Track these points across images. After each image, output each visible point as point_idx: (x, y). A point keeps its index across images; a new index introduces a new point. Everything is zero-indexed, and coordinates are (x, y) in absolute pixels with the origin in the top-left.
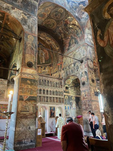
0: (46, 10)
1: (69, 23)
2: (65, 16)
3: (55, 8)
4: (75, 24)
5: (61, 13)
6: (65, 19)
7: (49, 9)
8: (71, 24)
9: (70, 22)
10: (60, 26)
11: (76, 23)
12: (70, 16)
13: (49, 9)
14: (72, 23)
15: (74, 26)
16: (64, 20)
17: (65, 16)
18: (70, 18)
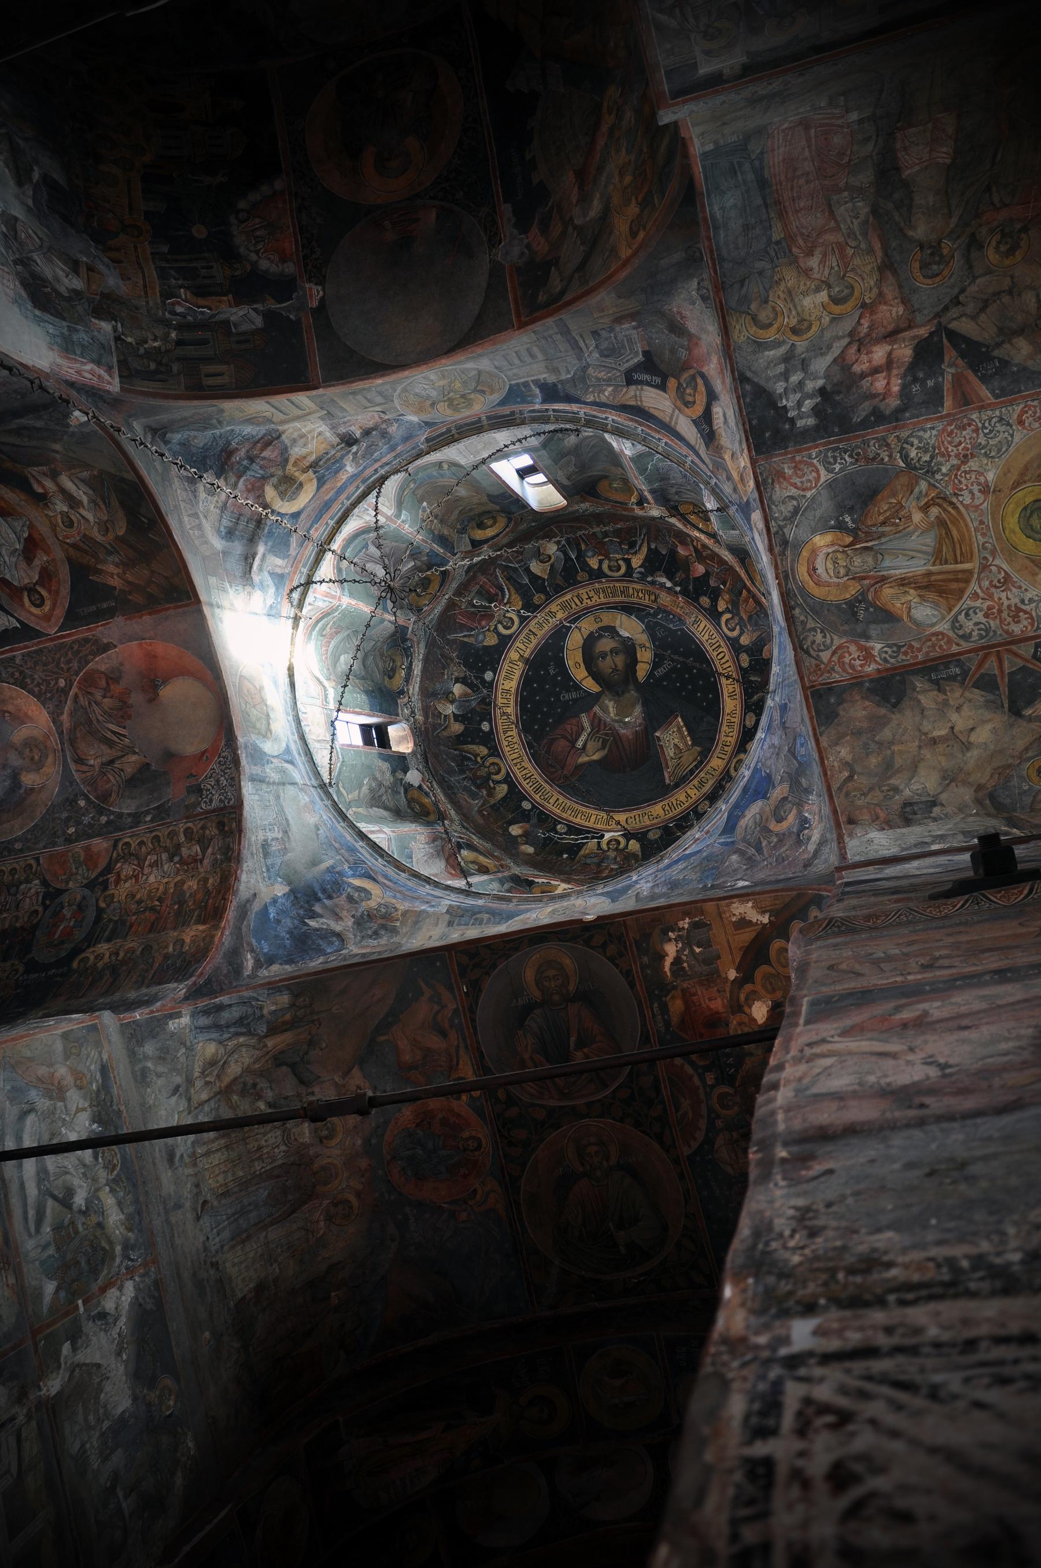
0: (407, 1058)
1: (718, 1005)
2: (632, 985)
3: (476, 987)
4: (746, 936)
5: (572, 988)
6: (664, 1008)
7: (434, 1042)
8: (739, 983)
9: (712, 978)
10: (703, 1124)
11: (743, 923)
12: (665, 932)
13: (434, 1042)
14: (732, 974)
15: (768, 962)
16: (667, 1024)
17: (632, 985)
18: (671, 950)
